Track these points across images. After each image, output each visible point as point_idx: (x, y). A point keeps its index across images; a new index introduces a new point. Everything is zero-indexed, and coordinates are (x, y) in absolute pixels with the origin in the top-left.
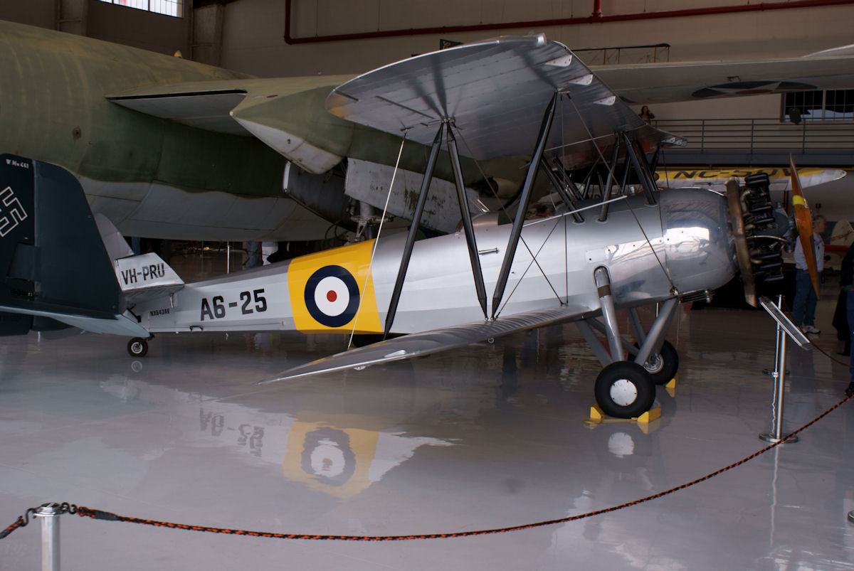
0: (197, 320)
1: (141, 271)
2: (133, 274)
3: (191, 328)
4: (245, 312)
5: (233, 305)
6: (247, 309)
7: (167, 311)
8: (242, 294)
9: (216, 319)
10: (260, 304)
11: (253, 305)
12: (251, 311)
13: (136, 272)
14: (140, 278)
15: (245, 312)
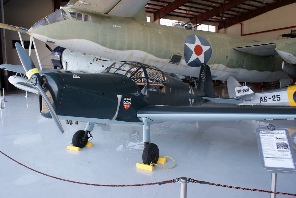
0: (259, 102)
1: (243, 90)
2: (240, 91)
3: (257, 104)
4: (273, 101)
5: (270, 99)
6: (274, 100)
7: (250, 100)
8: (273, 96)
9: (264, 102)
10: (278, 99)
11: (276, 99)
12: (275, 101)
13: (241, 90)
14: (242, 92)
15: (273, 101)
